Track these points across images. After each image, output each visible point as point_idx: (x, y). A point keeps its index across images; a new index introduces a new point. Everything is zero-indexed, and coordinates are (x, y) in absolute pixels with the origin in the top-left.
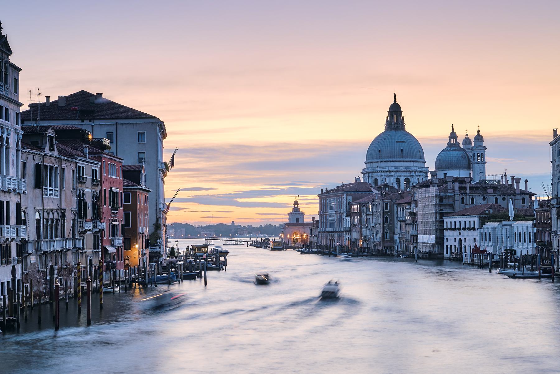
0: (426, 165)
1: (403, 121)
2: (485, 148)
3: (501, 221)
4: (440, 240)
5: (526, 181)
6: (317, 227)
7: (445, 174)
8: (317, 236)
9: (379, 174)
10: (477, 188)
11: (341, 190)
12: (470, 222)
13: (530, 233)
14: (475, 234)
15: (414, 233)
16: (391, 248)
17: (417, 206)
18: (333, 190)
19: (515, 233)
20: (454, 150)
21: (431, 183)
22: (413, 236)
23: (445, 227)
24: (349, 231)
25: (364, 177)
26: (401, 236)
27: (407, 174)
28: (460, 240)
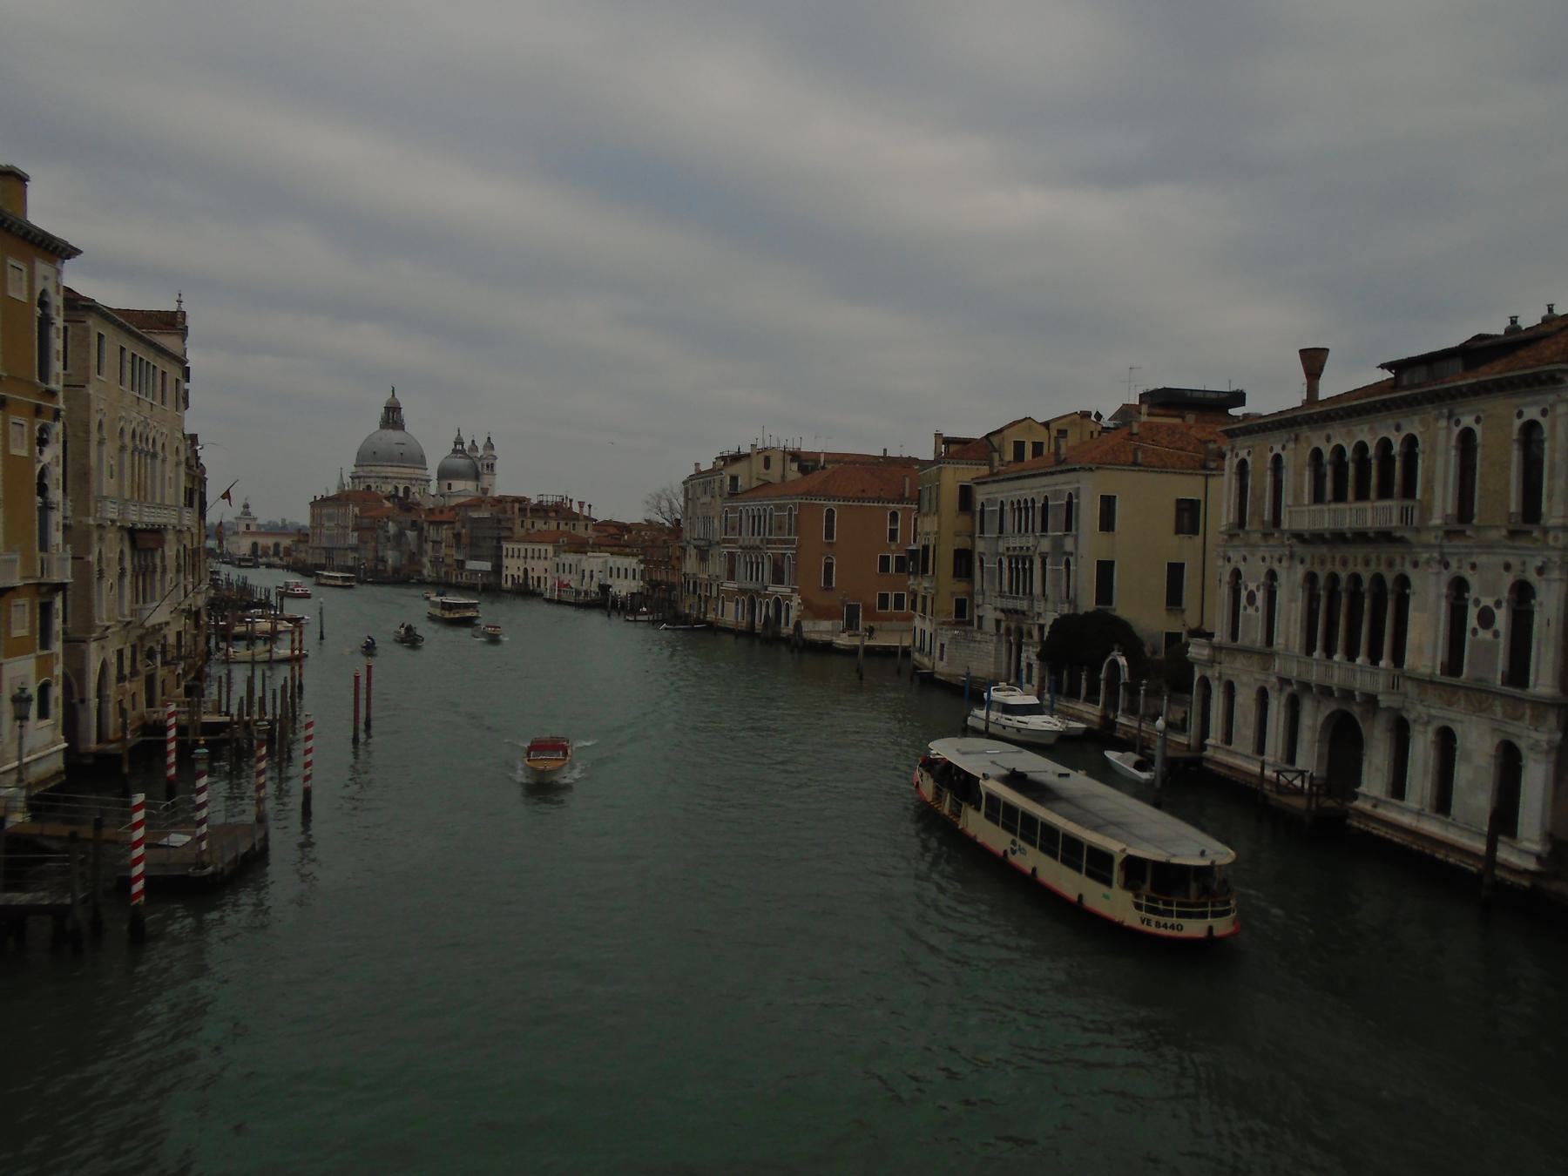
0: (428, 472)
1: (403, 421)
2: (495, 458)
3: (586, 553)
4: (498, 569)
5: (590, 506)
6: (307, 542)
7: (450, 485)
8: (307, 552)
9: (372, 480)
10: (537, 510)
11: (341, 499)
12: (540, 550)
13: (634, 570)
14: (547, 564)
15: (461, 558)
16: (420, 572)
17: (463, 527)
18: (328, 499)
19: (611, 568)
20: (460, 457)
21: (483, 502)
22: (457, 561)
23: (504, 553)
24: (354, 549)
25: (353, 483)
26: (433, 559)
27: (408, 482)
28: (526, 570)
